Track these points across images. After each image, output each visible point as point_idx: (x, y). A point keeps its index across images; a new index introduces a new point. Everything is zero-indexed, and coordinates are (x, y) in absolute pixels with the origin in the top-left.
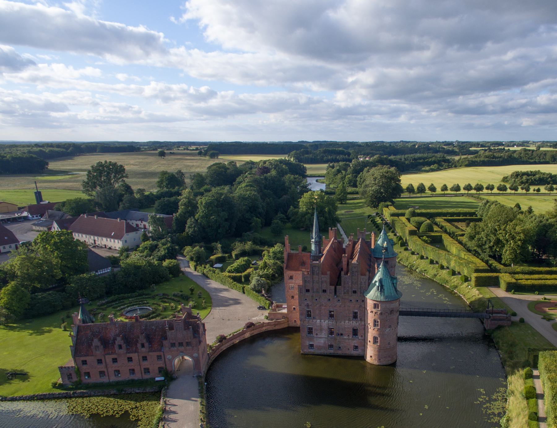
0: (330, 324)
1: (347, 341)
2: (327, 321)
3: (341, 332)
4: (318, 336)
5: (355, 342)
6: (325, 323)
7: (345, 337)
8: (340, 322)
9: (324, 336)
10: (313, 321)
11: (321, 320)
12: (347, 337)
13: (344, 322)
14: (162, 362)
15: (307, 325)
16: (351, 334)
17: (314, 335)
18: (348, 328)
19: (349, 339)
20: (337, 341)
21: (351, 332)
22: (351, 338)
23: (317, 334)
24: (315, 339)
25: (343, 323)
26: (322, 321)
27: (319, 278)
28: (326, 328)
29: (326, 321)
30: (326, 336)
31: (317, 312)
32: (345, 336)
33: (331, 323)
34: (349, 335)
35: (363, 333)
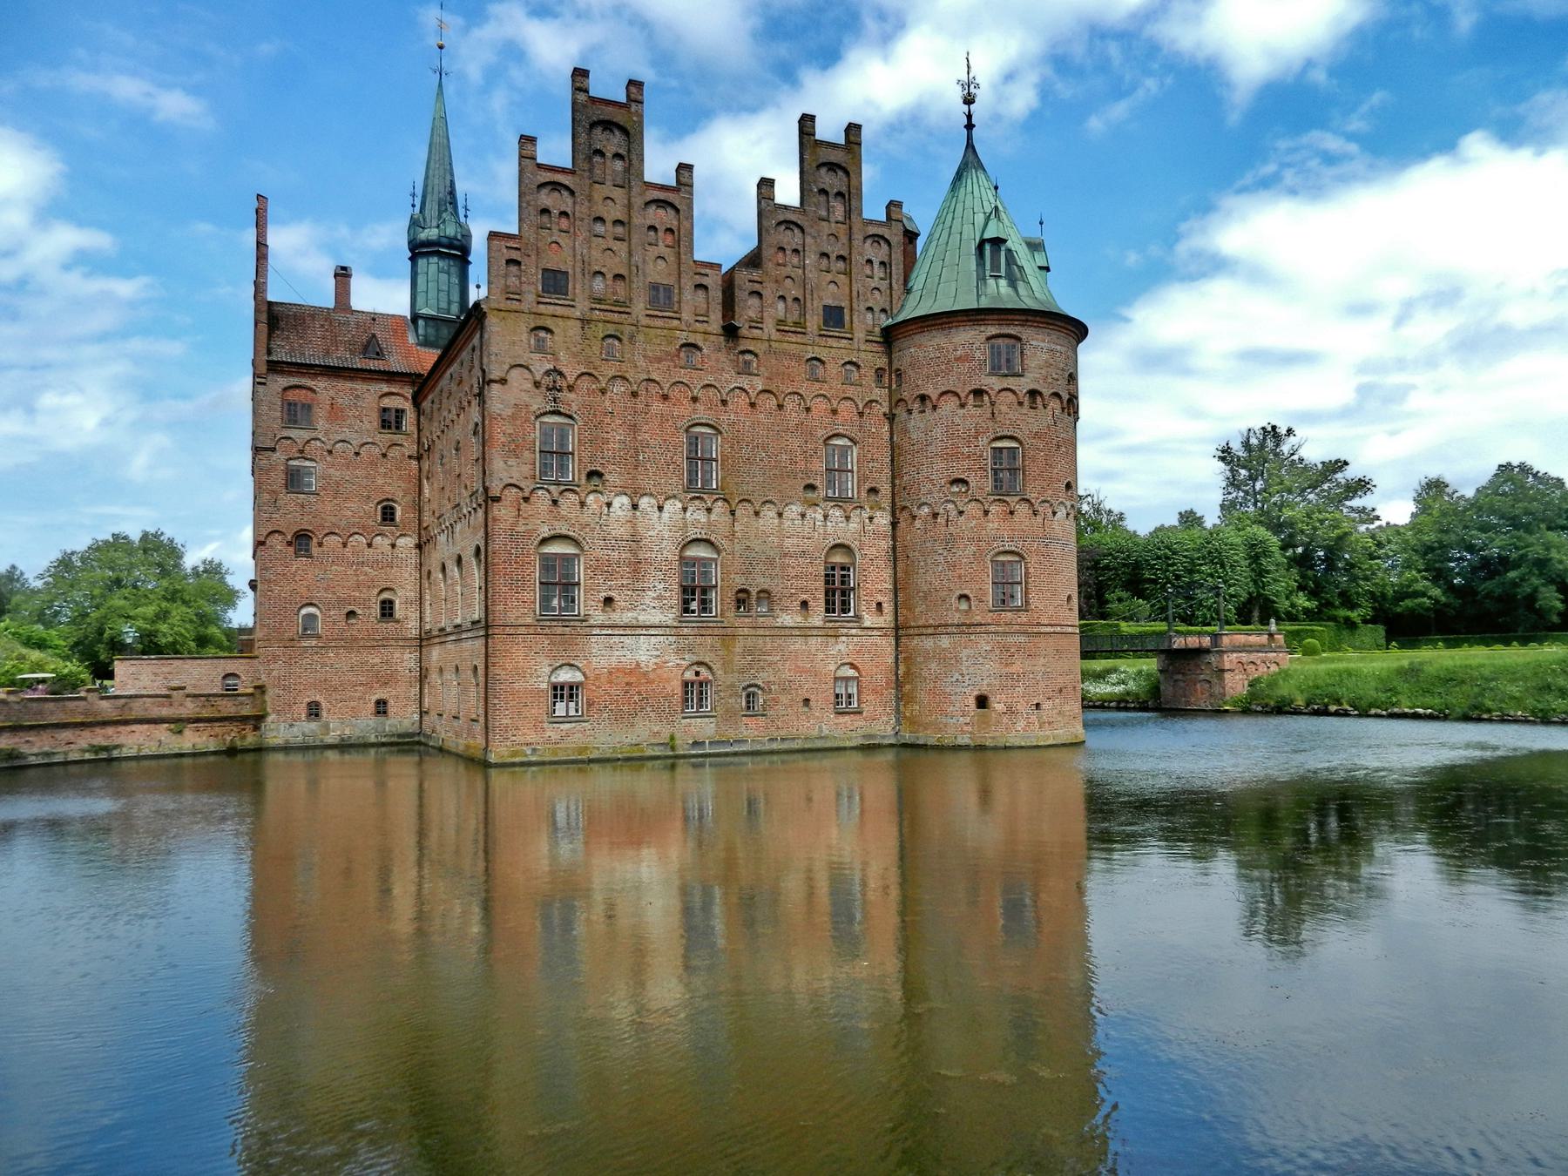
0: (695, 523)
1: (798, 645)
2: (672, 507)
3: (758, 582)
4: (618, 617)
5: (842, 647)
6: (665, 515)
7: (788, 619)
8: (757, 514)
9: (655, 617)
10: (582, 504)
11: (635, 495)
12: (799, 619)
13: (780, 515)
15: (545, 531)
16: (822, 596)
17: (587, 603)
19: (805, 632)
20: (738, 647)
21: (821, 584)
22: (817, 618)
23: (608, 601)
24: (596, 645)
25: (769, 513)
26: (645, 502)
27: (629, 206)
28: (669, 552)
29: (668, 506)
30: (669, 617)
31: (617, 436)
32: (785, 609)
33: (701, 516)
34: (804, 604)
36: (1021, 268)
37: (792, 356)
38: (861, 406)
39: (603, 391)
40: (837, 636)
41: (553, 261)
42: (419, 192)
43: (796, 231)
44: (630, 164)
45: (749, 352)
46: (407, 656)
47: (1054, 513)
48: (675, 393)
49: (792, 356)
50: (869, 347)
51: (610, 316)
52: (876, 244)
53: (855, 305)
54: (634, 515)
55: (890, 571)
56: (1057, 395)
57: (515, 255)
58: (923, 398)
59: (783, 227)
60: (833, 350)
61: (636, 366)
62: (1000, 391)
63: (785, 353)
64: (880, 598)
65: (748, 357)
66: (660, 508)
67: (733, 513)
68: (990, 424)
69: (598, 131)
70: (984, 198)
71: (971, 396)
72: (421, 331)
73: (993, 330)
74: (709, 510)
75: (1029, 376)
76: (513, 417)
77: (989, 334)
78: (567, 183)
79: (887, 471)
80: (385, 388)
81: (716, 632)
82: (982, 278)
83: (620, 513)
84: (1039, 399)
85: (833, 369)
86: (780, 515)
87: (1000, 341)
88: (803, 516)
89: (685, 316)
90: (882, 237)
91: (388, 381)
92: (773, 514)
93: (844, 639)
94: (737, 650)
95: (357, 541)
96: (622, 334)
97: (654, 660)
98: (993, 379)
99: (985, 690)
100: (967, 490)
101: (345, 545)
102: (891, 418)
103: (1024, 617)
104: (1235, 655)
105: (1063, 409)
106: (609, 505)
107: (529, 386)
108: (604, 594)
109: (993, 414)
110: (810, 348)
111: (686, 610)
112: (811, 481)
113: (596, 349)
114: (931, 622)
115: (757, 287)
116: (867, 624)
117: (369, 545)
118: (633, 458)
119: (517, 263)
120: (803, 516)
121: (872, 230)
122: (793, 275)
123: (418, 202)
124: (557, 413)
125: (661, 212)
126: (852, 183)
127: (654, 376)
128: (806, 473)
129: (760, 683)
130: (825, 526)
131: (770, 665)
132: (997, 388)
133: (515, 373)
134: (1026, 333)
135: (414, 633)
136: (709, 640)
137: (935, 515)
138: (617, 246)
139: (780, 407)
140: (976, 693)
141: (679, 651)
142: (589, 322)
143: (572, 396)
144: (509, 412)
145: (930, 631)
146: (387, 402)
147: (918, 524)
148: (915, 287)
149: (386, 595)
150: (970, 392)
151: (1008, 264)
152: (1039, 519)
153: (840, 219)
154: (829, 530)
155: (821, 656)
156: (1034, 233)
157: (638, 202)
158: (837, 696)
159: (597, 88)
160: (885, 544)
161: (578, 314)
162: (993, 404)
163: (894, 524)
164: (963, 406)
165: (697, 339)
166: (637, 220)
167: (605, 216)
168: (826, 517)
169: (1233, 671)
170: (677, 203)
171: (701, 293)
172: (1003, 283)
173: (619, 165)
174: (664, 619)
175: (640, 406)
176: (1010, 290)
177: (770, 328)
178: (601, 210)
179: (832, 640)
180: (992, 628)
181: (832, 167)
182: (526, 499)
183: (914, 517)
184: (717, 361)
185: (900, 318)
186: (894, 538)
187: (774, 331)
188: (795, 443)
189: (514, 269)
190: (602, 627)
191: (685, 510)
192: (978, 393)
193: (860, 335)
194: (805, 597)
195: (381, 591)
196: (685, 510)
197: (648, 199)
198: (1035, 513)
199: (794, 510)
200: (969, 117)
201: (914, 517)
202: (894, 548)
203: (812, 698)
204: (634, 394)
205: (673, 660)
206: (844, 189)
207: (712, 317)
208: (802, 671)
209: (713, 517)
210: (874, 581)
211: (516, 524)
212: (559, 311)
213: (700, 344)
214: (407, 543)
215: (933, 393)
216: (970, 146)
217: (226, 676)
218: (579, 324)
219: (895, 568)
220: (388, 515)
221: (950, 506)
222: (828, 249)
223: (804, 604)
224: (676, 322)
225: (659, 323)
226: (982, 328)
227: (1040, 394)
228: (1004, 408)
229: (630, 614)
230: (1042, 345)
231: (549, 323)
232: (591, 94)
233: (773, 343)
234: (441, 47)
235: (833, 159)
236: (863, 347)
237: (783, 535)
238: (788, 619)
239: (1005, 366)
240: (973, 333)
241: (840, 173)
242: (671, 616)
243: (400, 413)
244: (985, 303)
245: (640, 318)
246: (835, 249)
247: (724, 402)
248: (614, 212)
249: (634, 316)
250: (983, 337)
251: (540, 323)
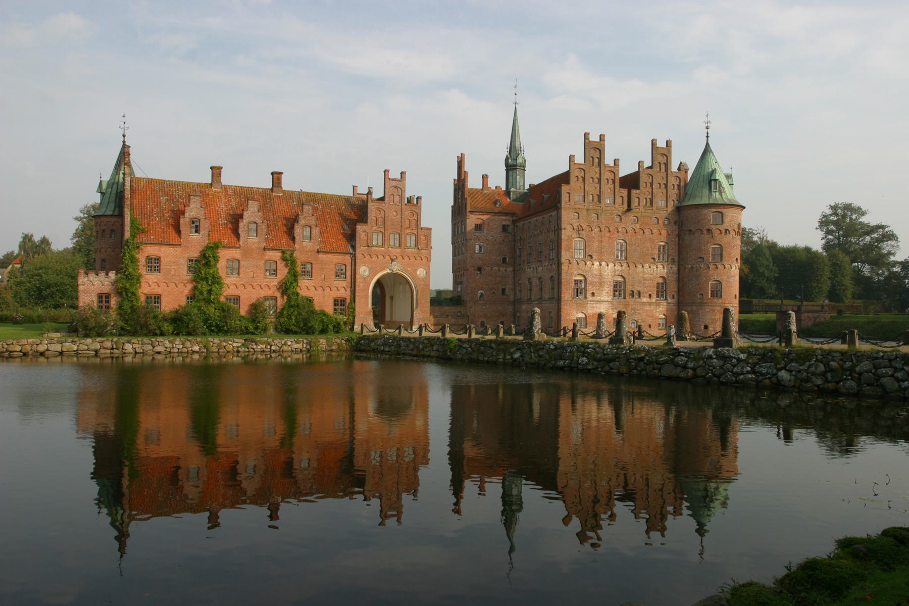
0: (618, 270)
1: (647, 308)
2: (611, 265)
3: (637, 288)
4: (595, 298)
5: (661, 309)
6: (609, 267)
7: (645, 300)
9: (606, 299)
10: (586, 264)
12: (648, 300)
13: (643, 267)
14: (344, 284)
15: (576, 273)
16: (655, 293)
18: (650, 280)
19: (650, 304)
21: (655, 289)
22: (654, 300)
26: (603, 264)
30: (610, 299)
32: (644, 297)
33: (620, 268)
35: (676, 290)
36: (723, 188)
38: (669, 232)
40: (660, 305)
42: (509, 146)
43: (651, 177)
46: (510, 307)
47: (731, 268)
54: (600, 268)
55: (677, 285)
56: (734, 230)
58: (690, 231)
64: (674, 293)
66: (608, 265)
67: (629, 266)
70: (712, 163)
72: (511, 196)
74: (622, 266)
76: (568, 239)
78: (583, 168)
79: (677, 253)
80: (504, 218)
81: (623, 303)
83: (596, 267)
84: (728, 232)
86: (643, 267)
88: (650, 267)
91: (505, 216)
92: (641, 267)
93: (662, 306)
94: (629, 309)
95: (495, 269)
97: (605, 311)
98: (713, 226)
99: (707, 324)
100: (703, 261)
101: (492, 270)
102: (679, 236)
103: (720, 301)
104: (807, 314)
105: (736, 234)
106: (593, 265)
108: (591, 292)
109: (712, 237)
111: (614, 296)
112: (653, 257)
114: (690, 302)
116: (669, 302)
117: (499, 270)
118: (600, 253)
120: (650, 267)
123: (509, 149)
124: (580, 238)
128: (652, 254)
129: (636, 319)
130: (657, 270)
131: (640, 313)
135: (512, 299)
136: (621, 306)
137: (693, 268)
139: (644, 233)
140: (704, 324)
141: (612, 309)
143: (584, 232)
144: (567, 238)
145: (690, 304)
146: (504, 223)
147: (687, 270)
148: (688, 193)
149: (503, 287)
151: (719, 187)
152: (726, 270)
154: (658, 272)
155: (654, 311)
156: (728, 172)
158: (659, 324)
159: (591, 139)
160: (675, 276)
163: (679, 270)
168: (657, 267)
169: (805, 320)
172: (717, 193)
174: (608, 299)
176: (720, 196)
179: (658, 307)
180: (710, 304)
182: (570, 263)
183: (685, 268)
184: (626, 220)
186: (679, 274)
188: (648, 245)
190: (591, 301)
191: (615, 266)
192: (708, 230)
194: (650, 293)
195: (502, 285)
196: (615, 266)
198: (725, 268)
199: (646, 266)
200: (707, 133)
201: (685, 268)
202: (679, 277)
203: (651, 324)
205: (611, 312)
208: (648, 316)
209: (623, 268)
210: (673, 288)
211: (568, 271)
214: (510, 269)
215: (692, 228)
216: (707, 144)
217: (458, 312)
219: (679, 284)
220: (504, 260)
221: (698, 265)
222: (660, 182)
223: (650, 296)
225: (609, 209)
226: (710, 209)
227: (728, 230)
228: (716, 235)
229: (599, 298)
232: (590, 140)
234: (516, 94)
237: (644, 273)
238: (645, 300)
242: (610, 298)
243: (508, 226)
244: (711, 202)
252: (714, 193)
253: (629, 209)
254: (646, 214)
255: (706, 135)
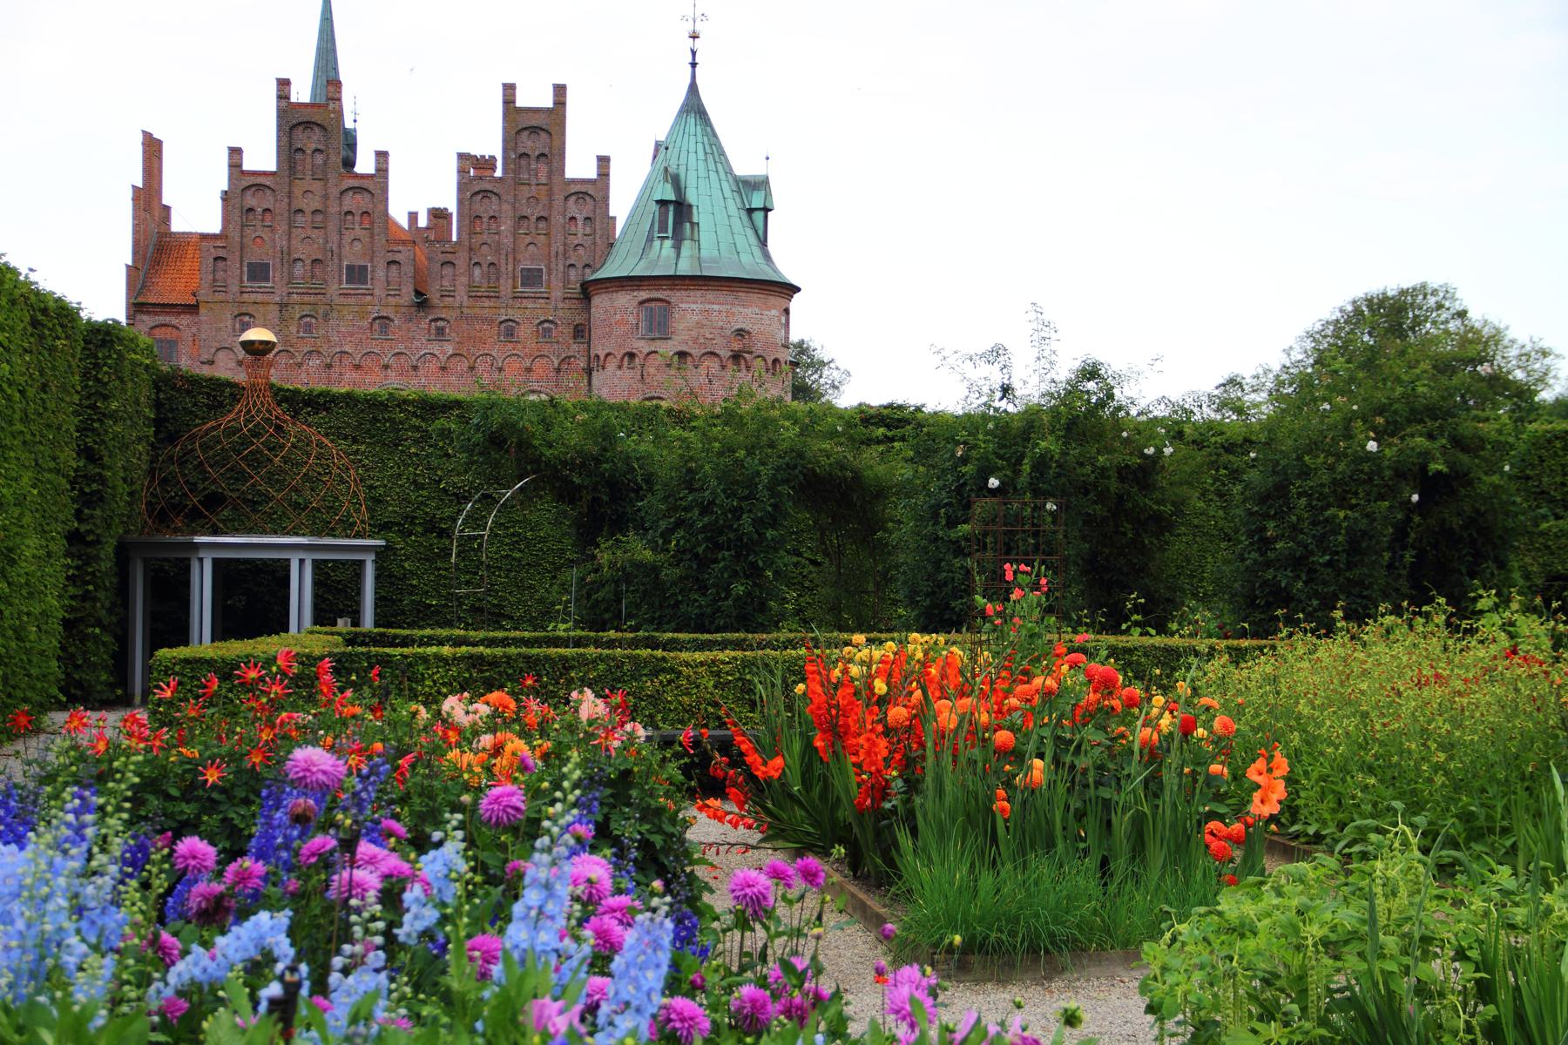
27: (326, 197)
37: (484, 320)
39: (300, 365)
41: (256, 255)
44: (328, 158)
45: (442, 319)
48: (368, 362)
49: (484, 320)
50: (568, 304)
51: (306, 298)
52: (581, 201)
53: (553, 266)
57: (221, 253)
59: (480, 196)
60: (528, 312)
61: (329, 341)
62: (649, 354)
63: (476, 317)
65: (440, 324)
68: (640, 386)
69: (299, 131)
71: (626, 359)
73: (644, 295)
75: (677, 338)
77: (640, 299)
82: (650, 240)
85: (525, 332)
87: (653, 304)
89: (377, 292)
90: (586, 193)
96: (317, 312)
98: (641, 344)
107: (233, 365)
110: (503, 311)
113: (293, 329)
115: (449, 257)
119: (224, 259)
121: (574, 189)
122: (489, 241)
125: (358, 196)
126: (554, 143)
127: (346, 349)
132: (646, 350)
133: (221, 355)
134: (675, 296)
138: (315, 234)
139: (472, 368)
142: (287, 305)
150: (625, 355)
153: (543, 180)
157: (335, 192)
161: (277, 299)
162: (643, 366)
164: (620, 367)
165: (391, 314)
166: (333, 209)
167: (304, 207)
170: (371, 188)
171: (394, 267)
172: (668, 243)
173: (319, 159)
175: (334, 376)
177: (461, 296)
178: (300, 203)
181: (534, 130)
185: (602, 274)
187: (466, 298)
189: (221, 264)
192: (632, 356)
193: (557, 293)
197: (344, 188)
200: (694, 53)
204: (329, 366)
206: (546, 151)
207: (404, 291)
212: (259, 297)
213: (392, 316)
216: (693, 88)
218: (277, 308)
224: (369, 298)
225: (352, 300)
228: (652, 370)
230: (694, 306)
231: (251, 309)
233: (465, 310)
235: (534, 123)
236: (561, 305)
239: (659, 326)
240: (628, 297)
241: (543, 135)
245: (335, 297)
246: (533, 212)
247: (415, 368)
248: (316, 204)
249: (328, 296)
250: (635, 303)
251: (244, 310)
252: (657, 243)
253: (422, 302)
254: (477, 311)
255: (690, 60)
